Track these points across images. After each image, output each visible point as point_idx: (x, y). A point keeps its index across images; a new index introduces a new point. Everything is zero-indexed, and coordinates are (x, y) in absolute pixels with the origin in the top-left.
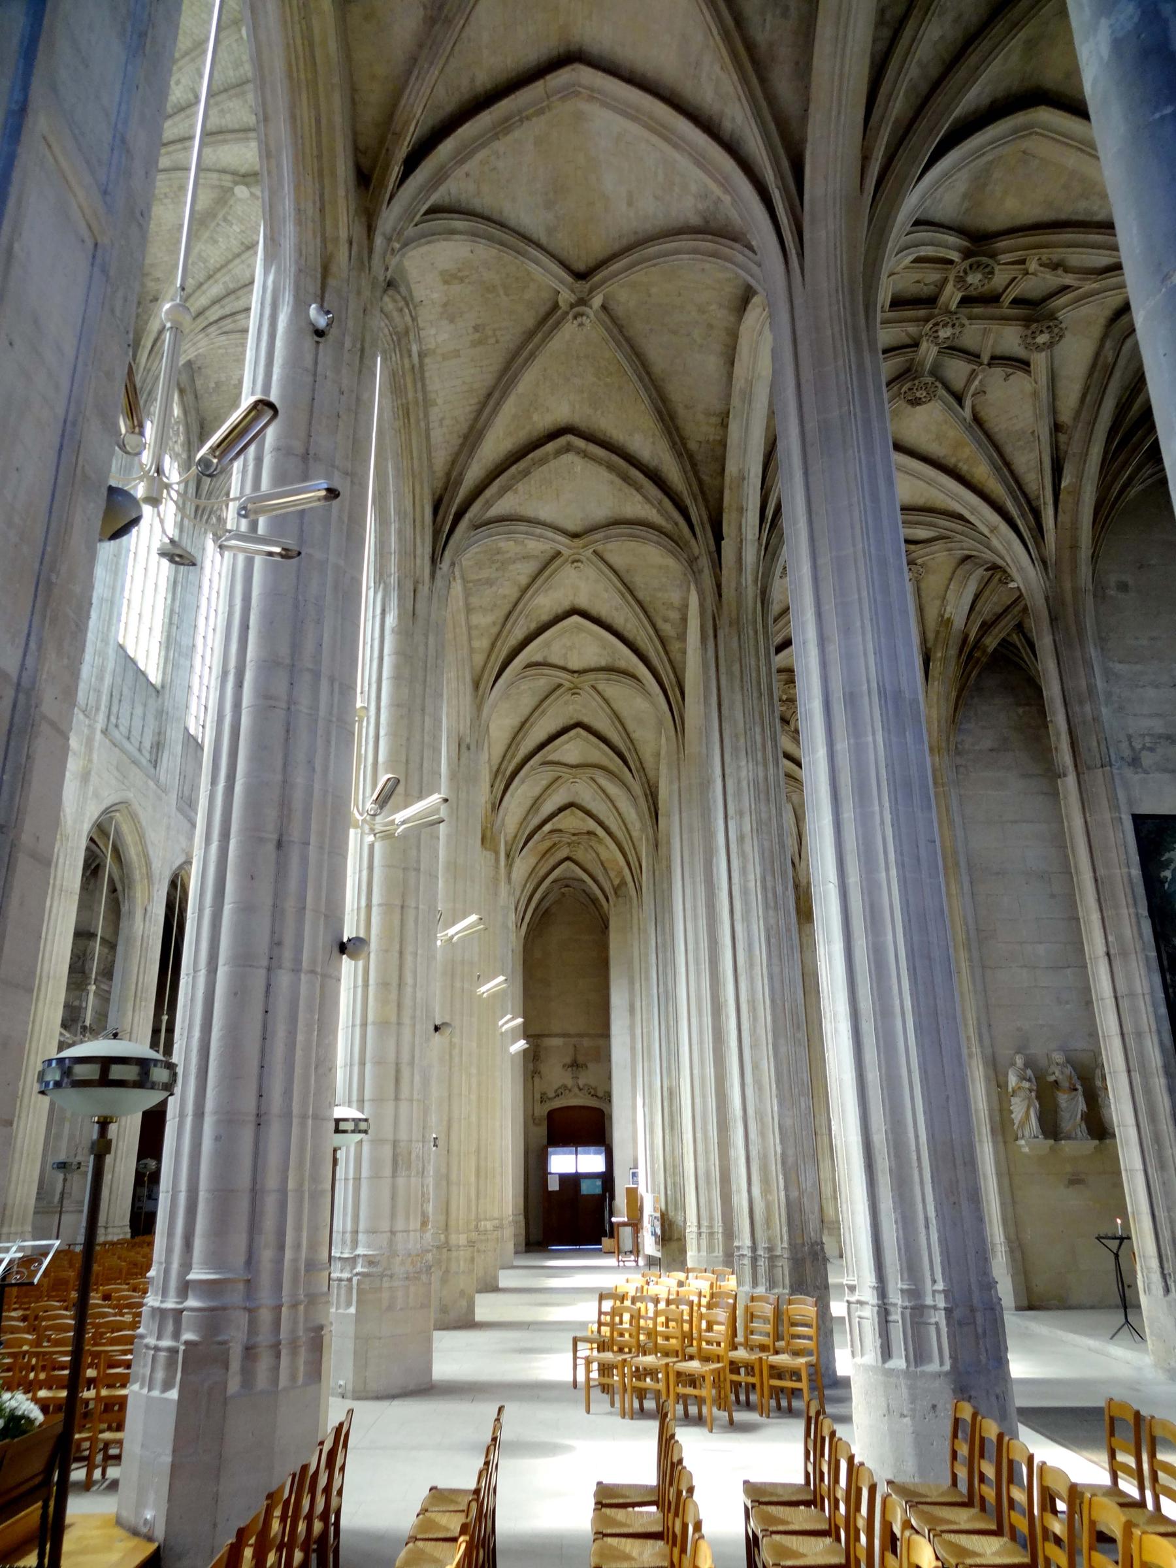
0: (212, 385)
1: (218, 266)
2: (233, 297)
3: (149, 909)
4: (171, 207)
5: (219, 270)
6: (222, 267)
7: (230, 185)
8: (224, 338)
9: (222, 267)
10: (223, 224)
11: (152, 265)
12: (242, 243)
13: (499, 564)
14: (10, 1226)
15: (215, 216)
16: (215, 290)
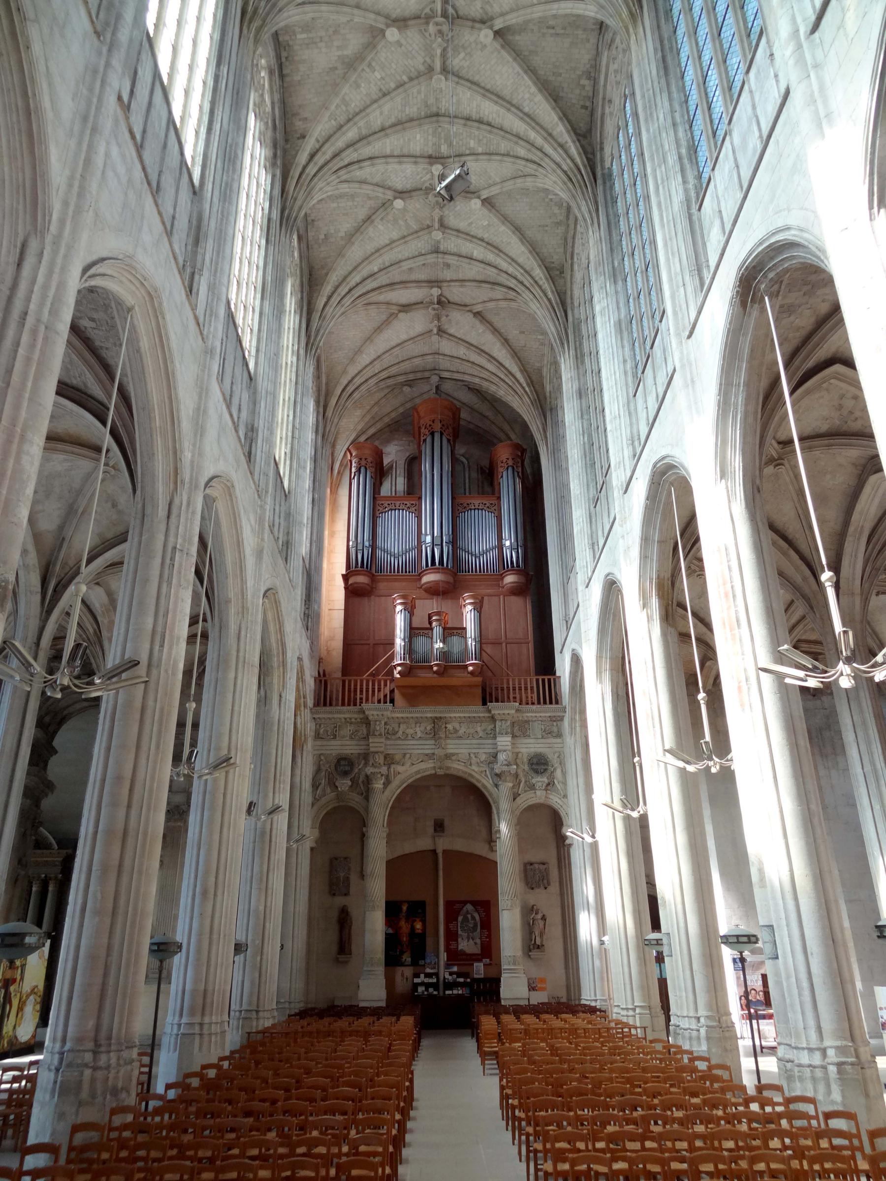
0: (322, 237)
1: (357, 110)
2: (365, 142)
3: (283, 695)
4: (324, 50)
5: (357, 114)
6: (361, 111)
7: (383, 26)
8: (345, 185)
9: (361, 111)
10: (367, 70)
11: (300, 106)
12: (381, 90)
13: (810, 287)
14: (211, 1015)
15: (363, 59)
16: (351, 134)
